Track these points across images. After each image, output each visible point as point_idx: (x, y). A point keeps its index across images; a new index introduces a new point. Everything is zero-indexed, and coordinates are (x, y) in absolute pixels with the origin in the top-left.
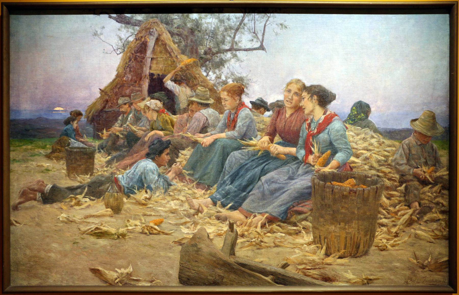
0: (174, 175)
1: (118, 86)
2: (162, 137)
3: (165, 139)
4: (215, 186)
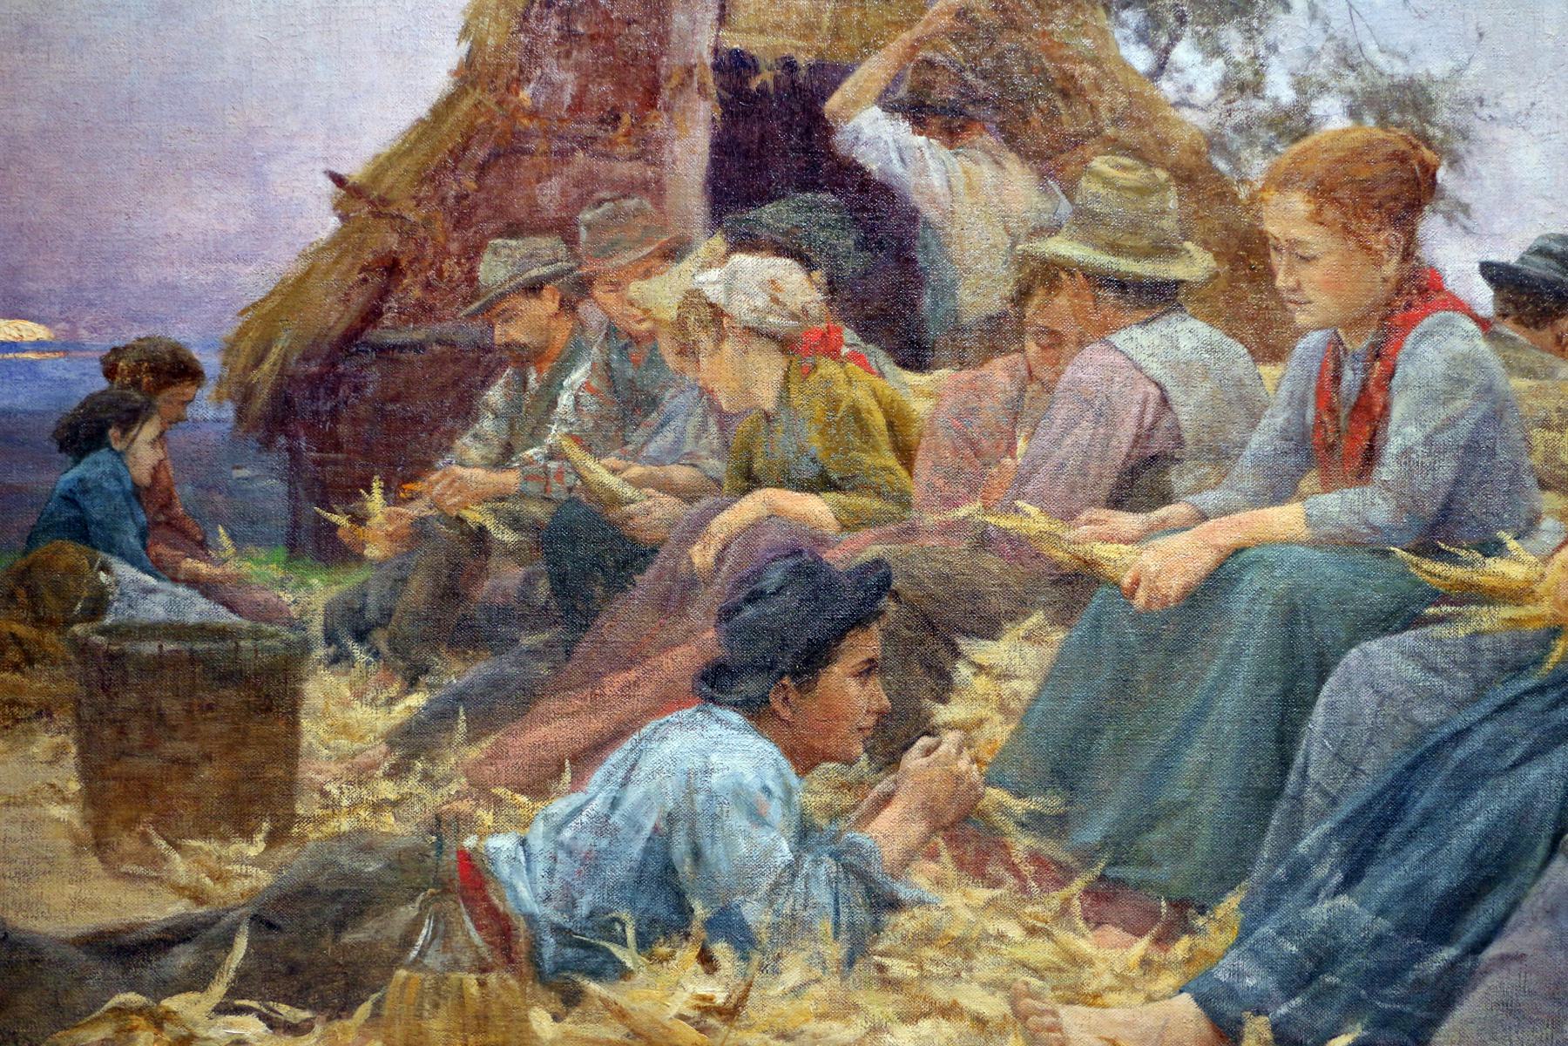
0: (917, 829)
1: (480, 153)
2: (821, 541)
3: (849, 553)
4: (1232, 901)
